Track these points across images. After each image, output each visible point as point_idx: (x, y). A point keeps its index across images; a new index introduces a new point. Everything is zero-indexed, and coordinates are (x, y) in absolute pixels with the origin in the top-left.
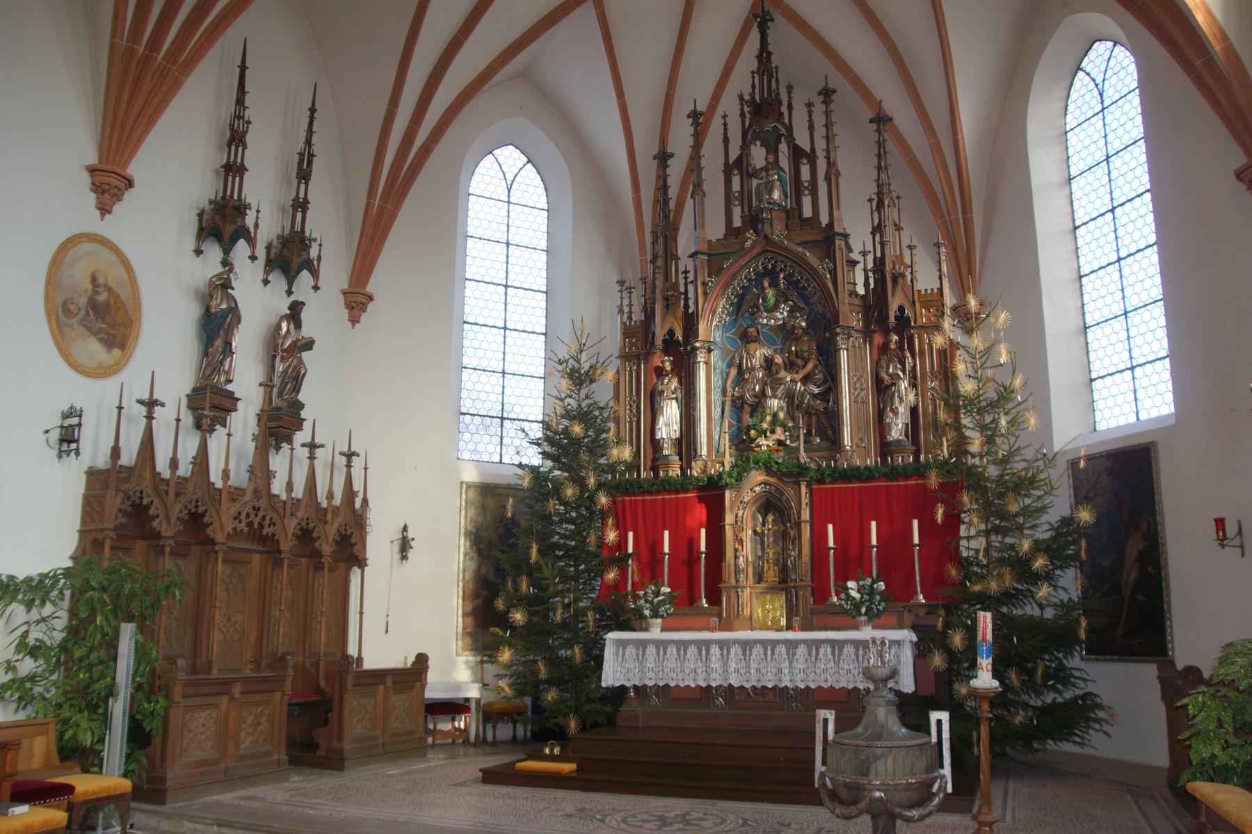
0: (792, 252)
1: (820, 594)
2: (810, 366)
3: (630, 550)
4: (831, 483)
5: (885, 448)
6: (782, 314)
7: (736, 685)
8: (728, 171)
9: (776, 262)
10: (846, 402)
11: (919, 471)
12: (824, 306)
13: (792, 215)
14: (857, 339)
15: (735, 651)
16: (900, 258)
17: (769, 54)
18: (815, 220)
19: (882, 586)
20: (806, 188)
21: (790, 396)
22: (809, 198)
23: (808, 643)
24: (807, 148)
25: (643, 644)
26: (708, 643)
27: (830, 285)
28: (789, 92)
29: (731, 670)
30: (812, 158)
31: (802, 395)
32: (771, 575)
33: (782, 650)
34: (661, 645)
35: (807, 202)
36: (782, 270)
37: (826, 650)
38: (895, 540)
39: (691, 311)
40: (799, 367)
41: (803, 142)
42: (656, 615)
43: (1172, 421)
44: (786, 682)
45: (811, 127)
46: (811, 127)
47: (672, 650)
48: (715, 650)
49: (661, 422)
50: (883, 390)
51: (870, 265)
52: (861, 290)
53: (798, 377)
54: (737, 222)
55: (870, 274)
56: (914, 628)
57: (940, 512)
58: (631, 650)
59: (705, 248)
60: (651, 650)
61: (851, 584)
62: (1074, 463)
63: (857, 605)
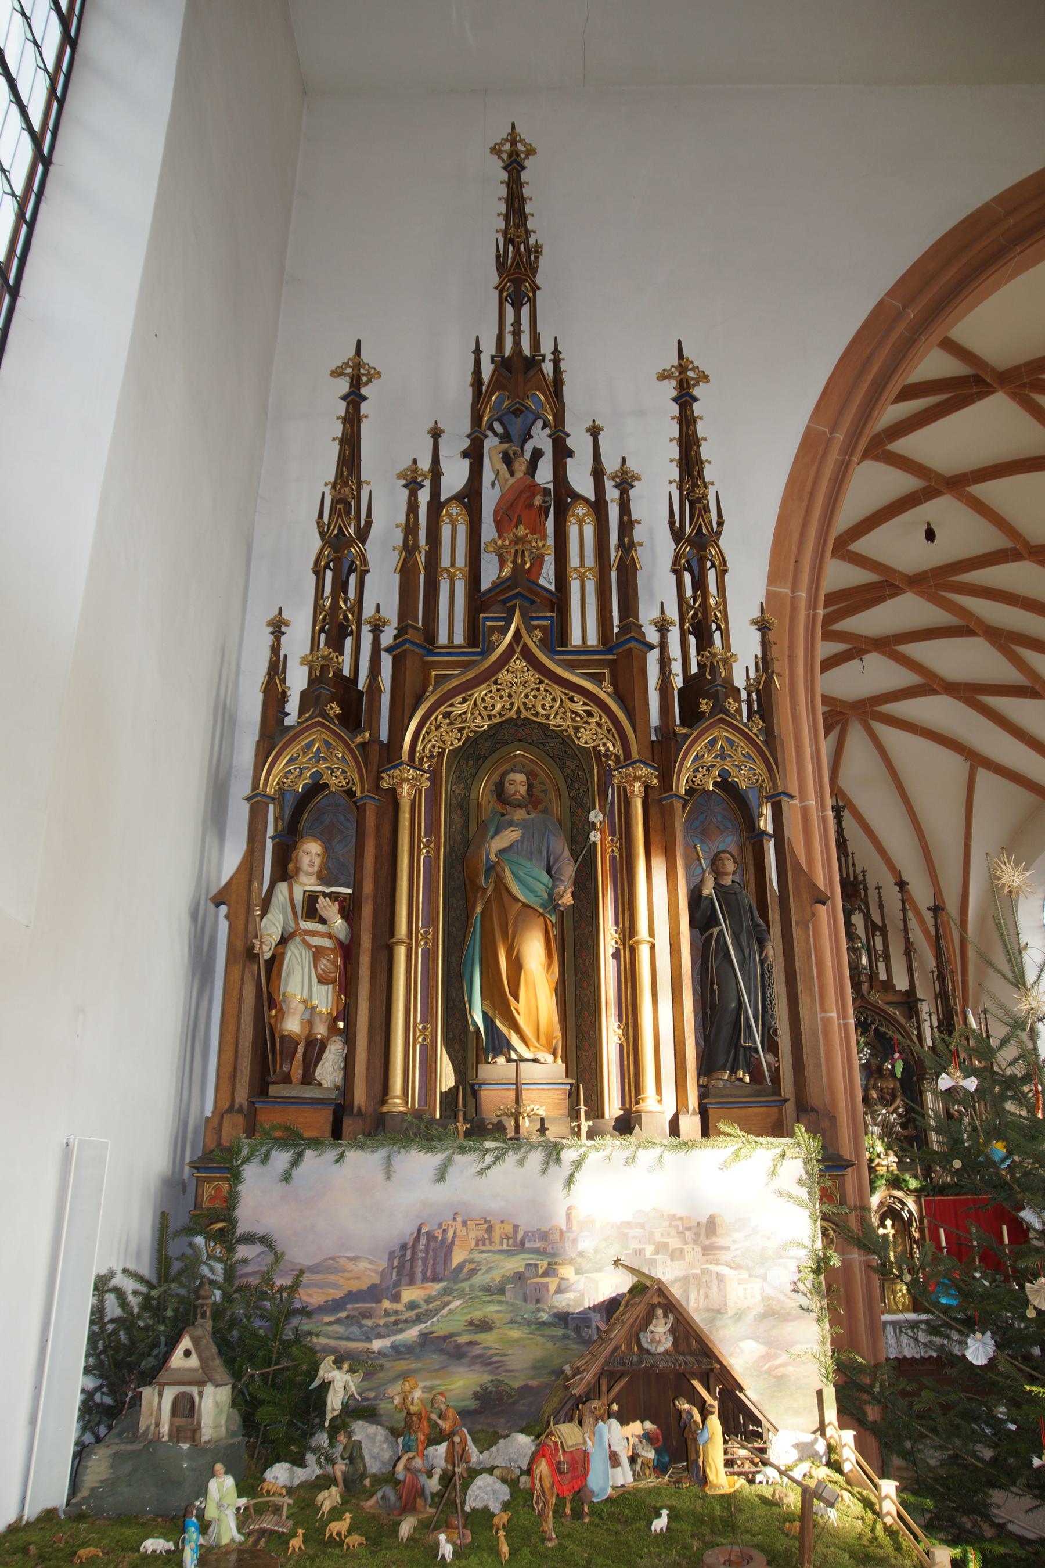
0: (884, 1011)
4: (933, 1196)
7: (909, 1356)
9: (867, 1015)
12: (907, 1055)
13: (873, 975)
17: (845, 841)
18: (888, 986)
20: (880, 956)
21: (885, 1125)
22: (883, 964)
24: (880, 924)
27: (915, 1039)
28: (864, 876)
29: (904, 1344)
31: (893, 1125)
35: (882, 967)
36: (873, 1023)
40: (887, 1101)
41: (877, 919)
51: (935, 1024)
52: (930, 1043)
53: (891, 1109)
55: (936, 1030)
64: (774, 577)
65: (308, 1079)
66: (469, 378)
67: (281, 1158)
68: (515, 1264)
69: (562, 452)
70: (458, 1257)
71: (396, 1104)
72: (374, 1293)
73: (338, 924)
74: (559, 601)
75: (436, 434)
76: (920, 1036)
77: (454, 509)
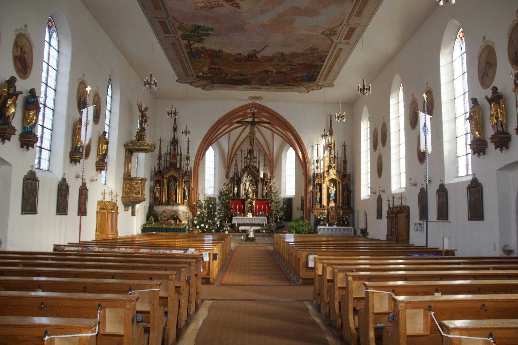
1: (256, 213)
2: (255, 186)
3: (233, 207)
5: (263, 197)
6: (251, 178)
8: (245, 158)
10: (259, 191)
11: (268, 200)
14: (260, 183)
15: (248, 220)
16: (266, 173)
18: (256, 167)
19: (264, 213)
21: (252, 190)
23: (257, 219)
24: (255, 157)
25: (237, 219)
26: (245, 219)
30: (256, 158)
32: (250, 211)
33: (253, 220)
34: (240, 219)
35: (255, 164)
37: (258, 220)
38: (265, 208)
39: (239, 176)
42: (238, 215)
43: (294, 196)
44: (254, 223)
45: (256, 154)
46: (256, 154)
47: (241, 219)
48: (246, 219)
49: (235, 191)
50: (263, 189)
54: (246, 165)
56: (267, 217)
57: (270, 205)
58: (236, 219)
59: (242, 169)
60: (238, 219)
61: (260, 213)
62: (284, 199)
63: (261, 215)
64: (196, 159)
65: (158, 200)
66: (170, 141)
67: (156, 206)
68: (169, 212)
69: (178, 149)
70: (166, 212)
71: (164, 202)
72: (161, 214)
73: (160, 190)
74: (176, 164)
75: (167, 147)
76: (259, 176)
77: (169, 155)
